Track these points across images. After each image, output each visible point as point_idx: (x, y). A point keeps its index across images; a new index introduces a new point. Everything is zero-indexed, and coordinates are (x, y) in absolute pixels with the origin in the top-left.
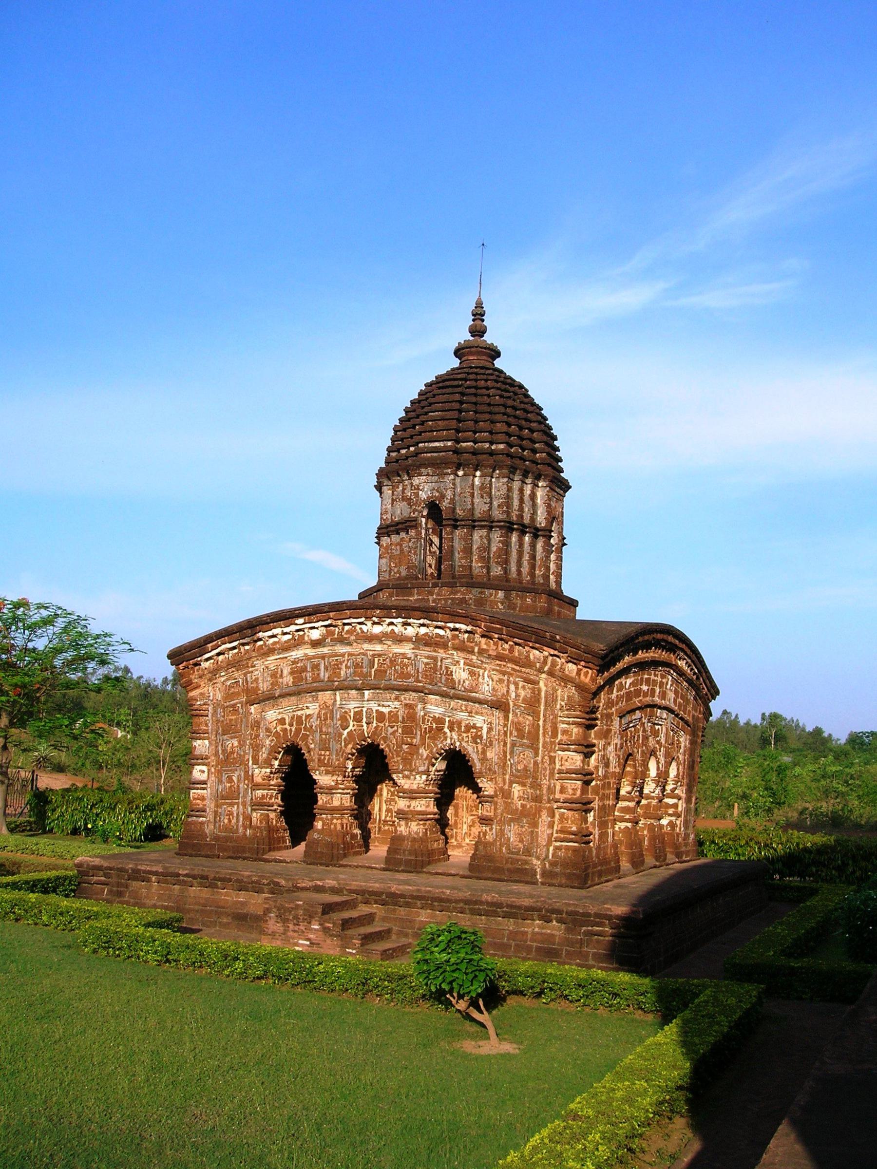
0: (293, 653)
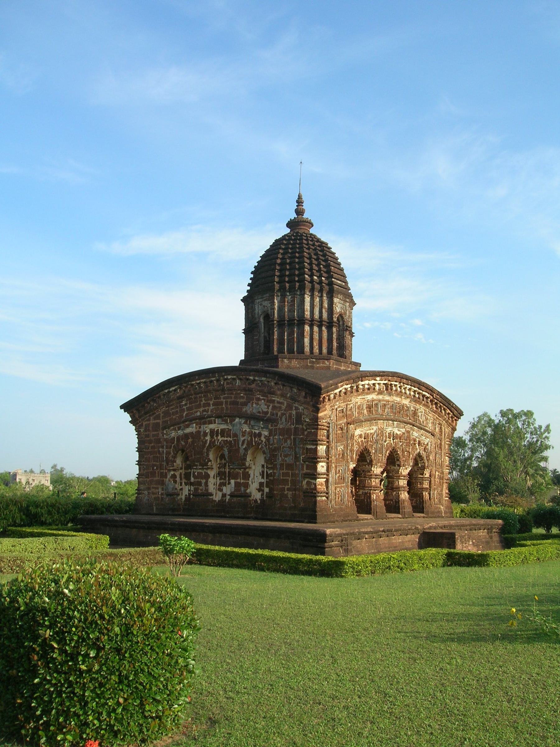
0: (368, 396)
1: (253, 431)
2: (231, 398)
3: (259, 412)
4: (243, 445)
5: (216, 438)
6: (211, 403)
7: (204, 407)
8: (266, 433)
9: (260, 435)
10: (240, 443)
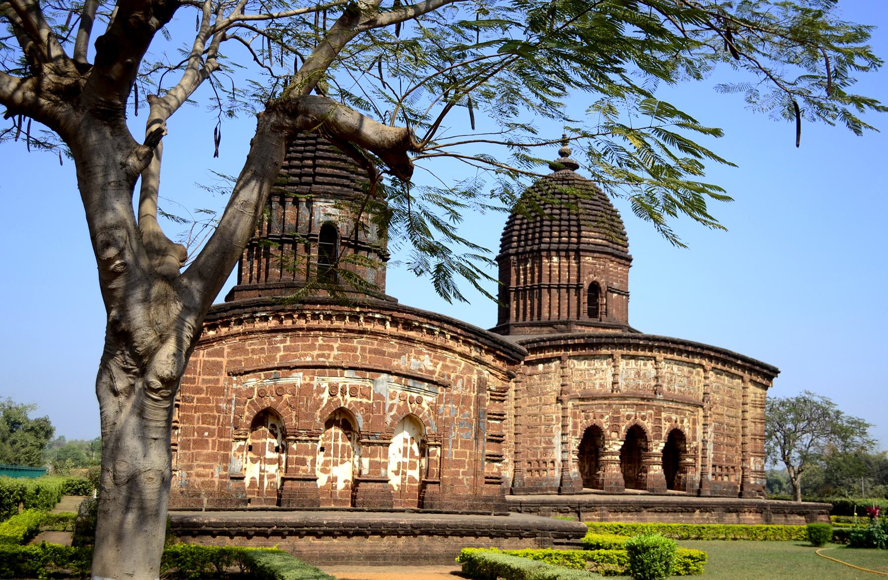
1: (408, 393)
2: (373, 344)
3: (420, 370)
4: (391, 410)
5: (341, 398)
6: (336, 345)
7: (319, 349)
8: (430, 399)
9: (419, 401)
10: (387, 408)
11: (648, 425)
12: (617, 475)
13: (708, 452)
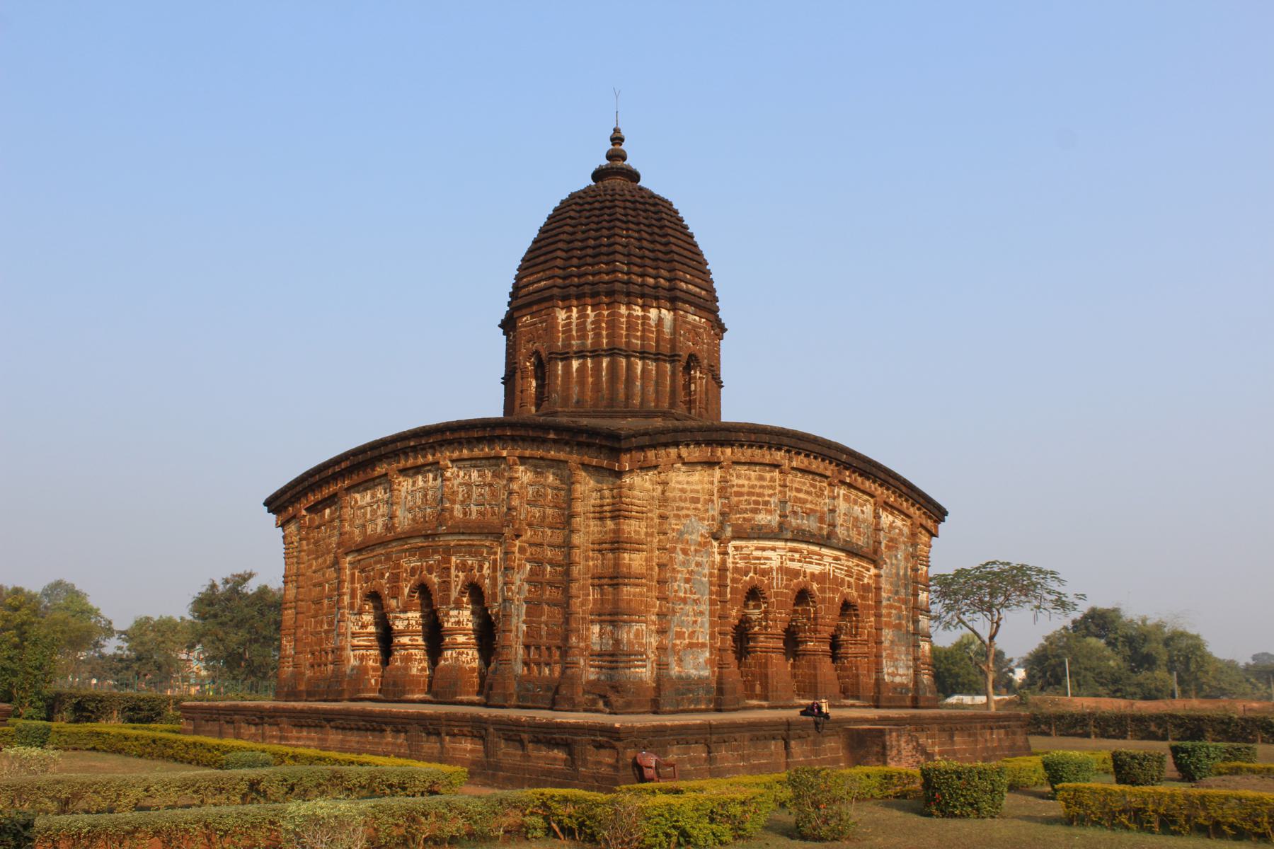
11: (435, 579)
12: (398, 668)
13: (514, 620)
